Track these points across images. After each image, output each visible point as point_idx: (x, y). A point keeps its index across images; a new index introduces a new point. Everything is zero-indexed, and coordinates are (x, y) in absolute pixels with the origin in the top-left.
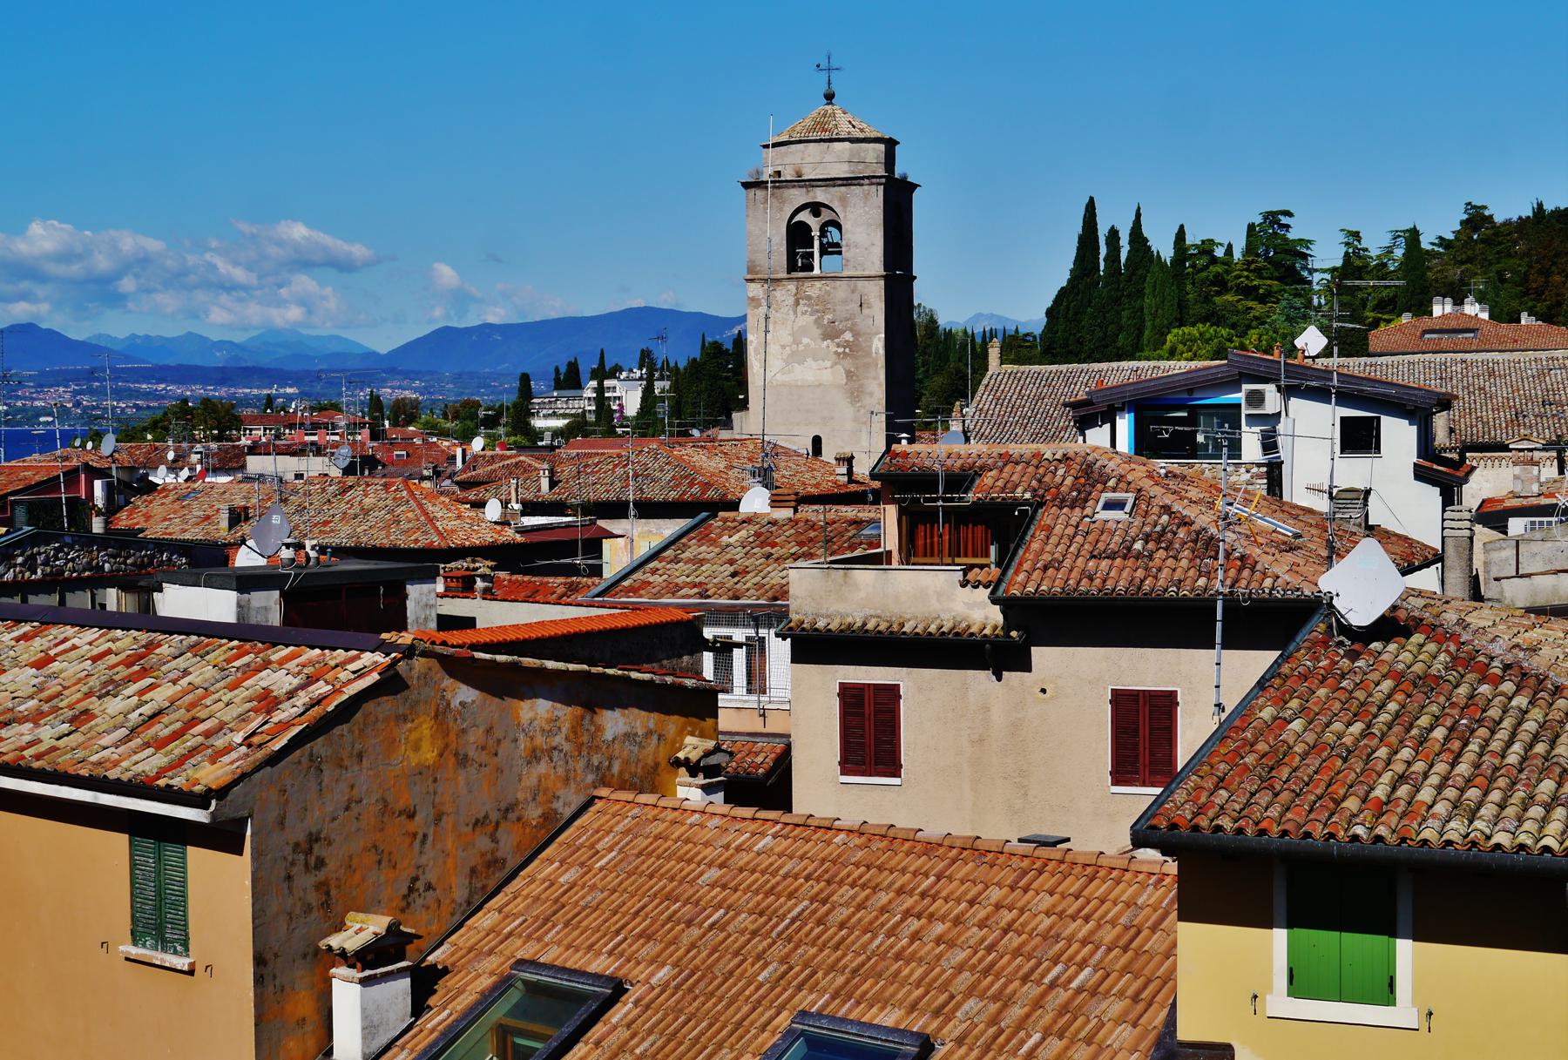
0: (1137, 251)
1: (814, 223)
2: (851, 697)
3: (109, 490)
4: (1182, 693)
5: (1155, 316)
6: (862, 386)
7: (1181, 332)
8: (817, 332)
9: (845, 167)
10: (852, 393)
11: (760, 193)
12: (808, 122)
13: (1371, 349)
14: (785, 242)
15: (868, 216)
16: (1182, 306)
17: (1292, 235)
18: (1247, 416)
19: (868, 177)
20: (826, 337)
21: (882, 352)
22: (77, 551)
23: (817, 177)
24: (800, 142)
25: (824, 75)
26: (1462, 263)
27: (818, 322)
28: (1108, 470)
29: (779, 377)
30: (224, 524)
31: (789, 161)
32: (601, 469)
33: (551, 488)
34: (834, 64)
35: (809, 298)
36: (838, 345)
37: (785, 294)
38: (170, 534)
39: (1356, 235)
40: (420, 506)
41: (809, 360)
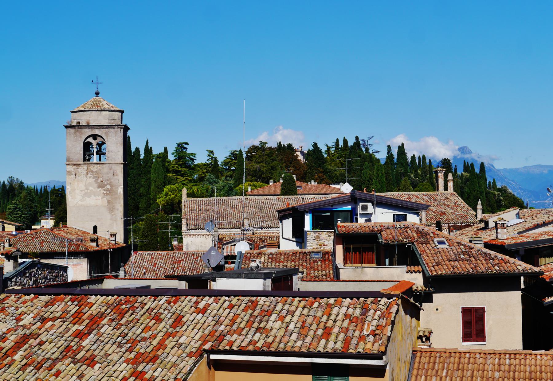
0: (147, 156)
1: (94, 143)
4: (487, 308)
6: (114, 206)
7: (169, 187)
8: (96, 185)
9: (107, 121)
10: (110, 209)
11: (72, 130)
12: (91, 103)
13: (298, 193)
14: (82, 150)
15: (117, 140)
17: (188, 152)
18: (360, 214)
19: (117, 125)
20: (99, 187)
21: (122, 193)
22: (41, 270)
23: (96, 125)
24: (89, 111)
25: (95, 85)
26: (259, 163)
27: (96, 181)
29: (80, 203)
31: (83, 119)
32: (26, 240)
34: (99, 81)
35: (92, 172)
36: (104, 190)
37: (83, 170)
39: (212, 152)
41: (93, 197)
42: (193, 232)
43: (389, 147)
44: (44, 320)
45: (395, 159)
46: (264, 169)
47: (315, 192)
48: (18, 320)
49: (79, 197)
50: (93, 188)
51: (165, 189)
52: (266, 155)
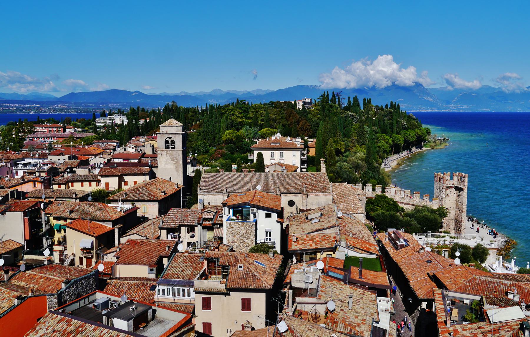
1: (170, 141)
2: (204, 299)
3: (44, 205)
5: (223, 127)
9: (175, 131)
16: (227, 128)
20: (172, 160)
21: (182, 163)
27: (170, 158)
28: (238, 258)
30: (68, 213)
33: (126, 196)
35: (169, 154)
37: (164, 153)
38: (58, 215)
40: (106, 209)
41: (169, 164)
42: (202, 193)
43: (349, 98)
44: (54, 331)
45: (352, 104)
46: (277, 118)
47: (285, 147)
48: (47, 329)
49: (163, 165)
50: (169, 161)
51: (226, 133)
52: (279, 111)
